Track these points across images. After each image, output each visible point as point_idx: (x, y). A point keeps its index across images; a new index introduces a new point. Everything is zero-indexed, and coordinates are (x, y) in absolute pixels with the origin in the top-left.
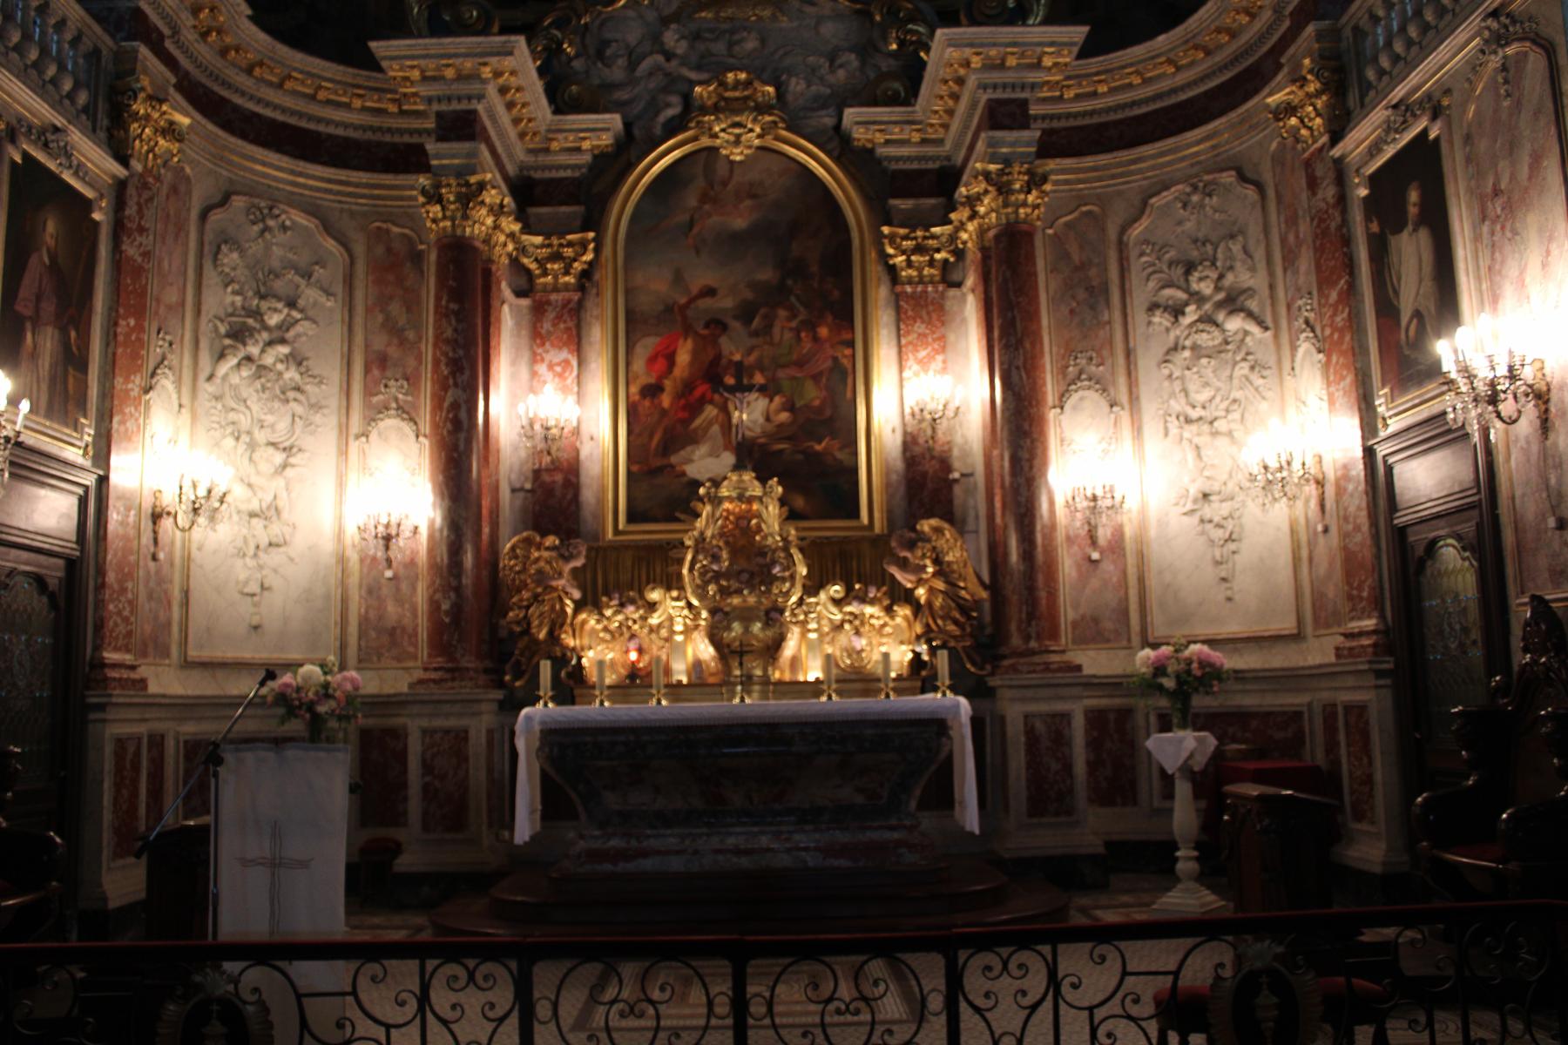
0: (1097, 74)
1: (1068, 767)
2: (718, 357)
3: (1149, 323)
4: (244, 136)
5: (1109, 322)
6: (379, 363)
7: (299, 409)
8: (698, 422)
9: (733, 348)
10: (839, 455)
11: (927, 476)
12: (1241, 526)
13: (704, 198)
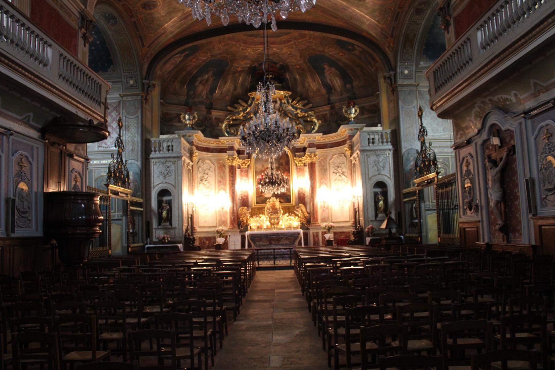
1: (319, 239)
6: (220, 182)
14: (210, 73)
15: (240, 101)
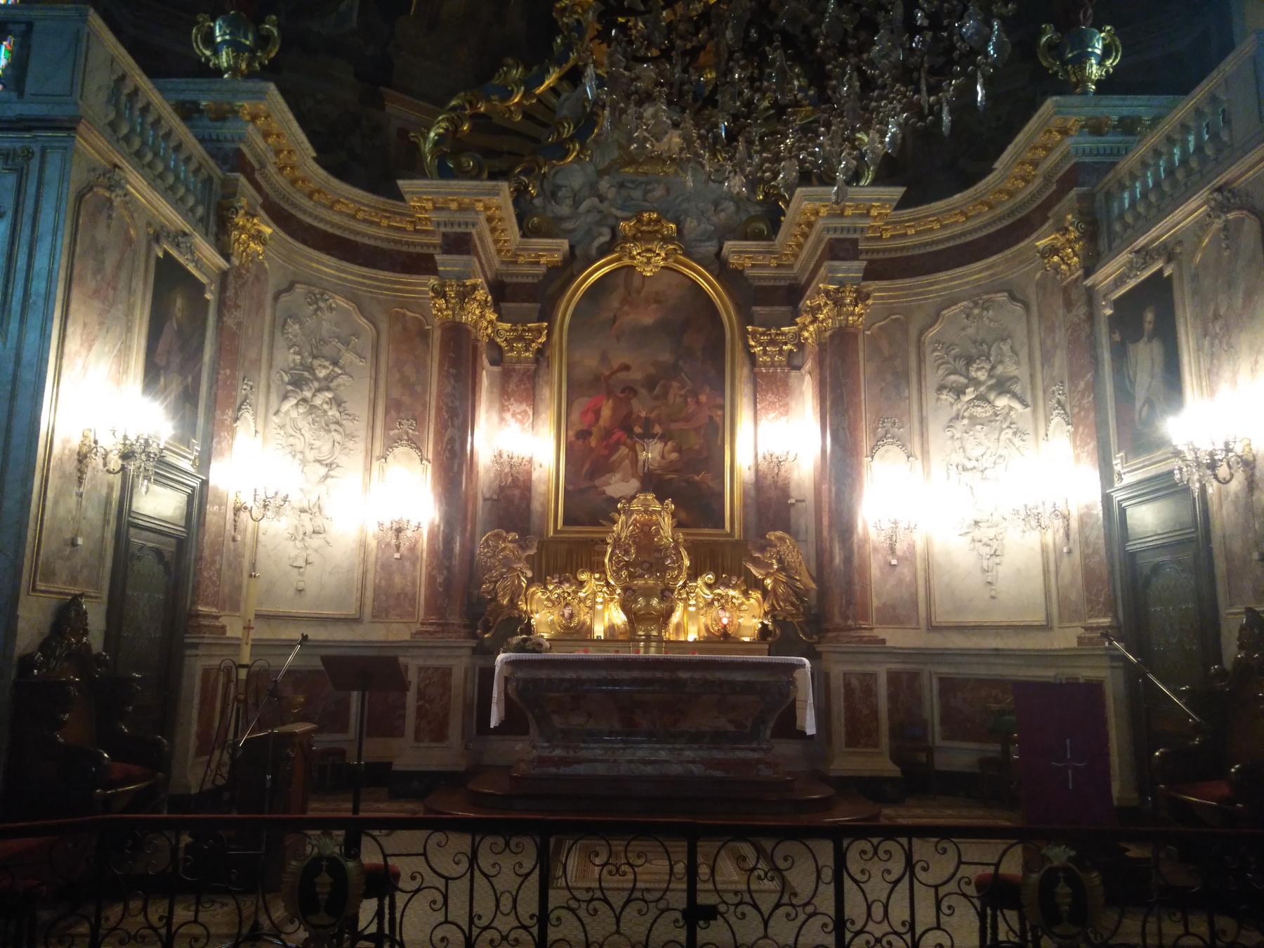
0: (908, 221)
2: (630, 413)
3: (938, 399)
4: (304, 242)
5: (909, 398)
6: (395, 408)
7: (338, 437)
8: (614, 458)
9: (641, 408)
10: (711, 484)
11: (772, 502)
12: (1003, 545)
13: (624, 301)
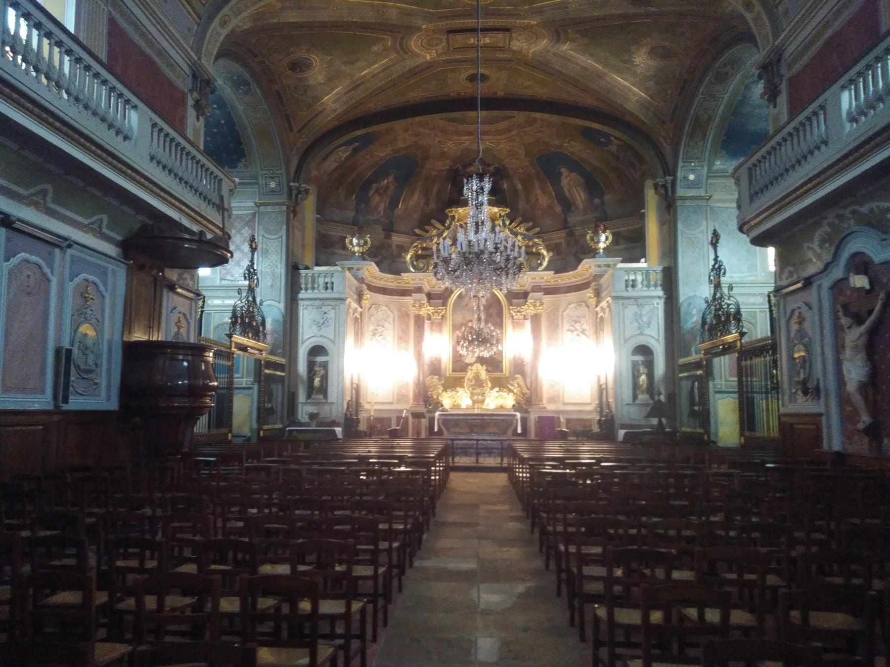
6: (400, 338)
14: (391, 178)
15: (433, 221)
